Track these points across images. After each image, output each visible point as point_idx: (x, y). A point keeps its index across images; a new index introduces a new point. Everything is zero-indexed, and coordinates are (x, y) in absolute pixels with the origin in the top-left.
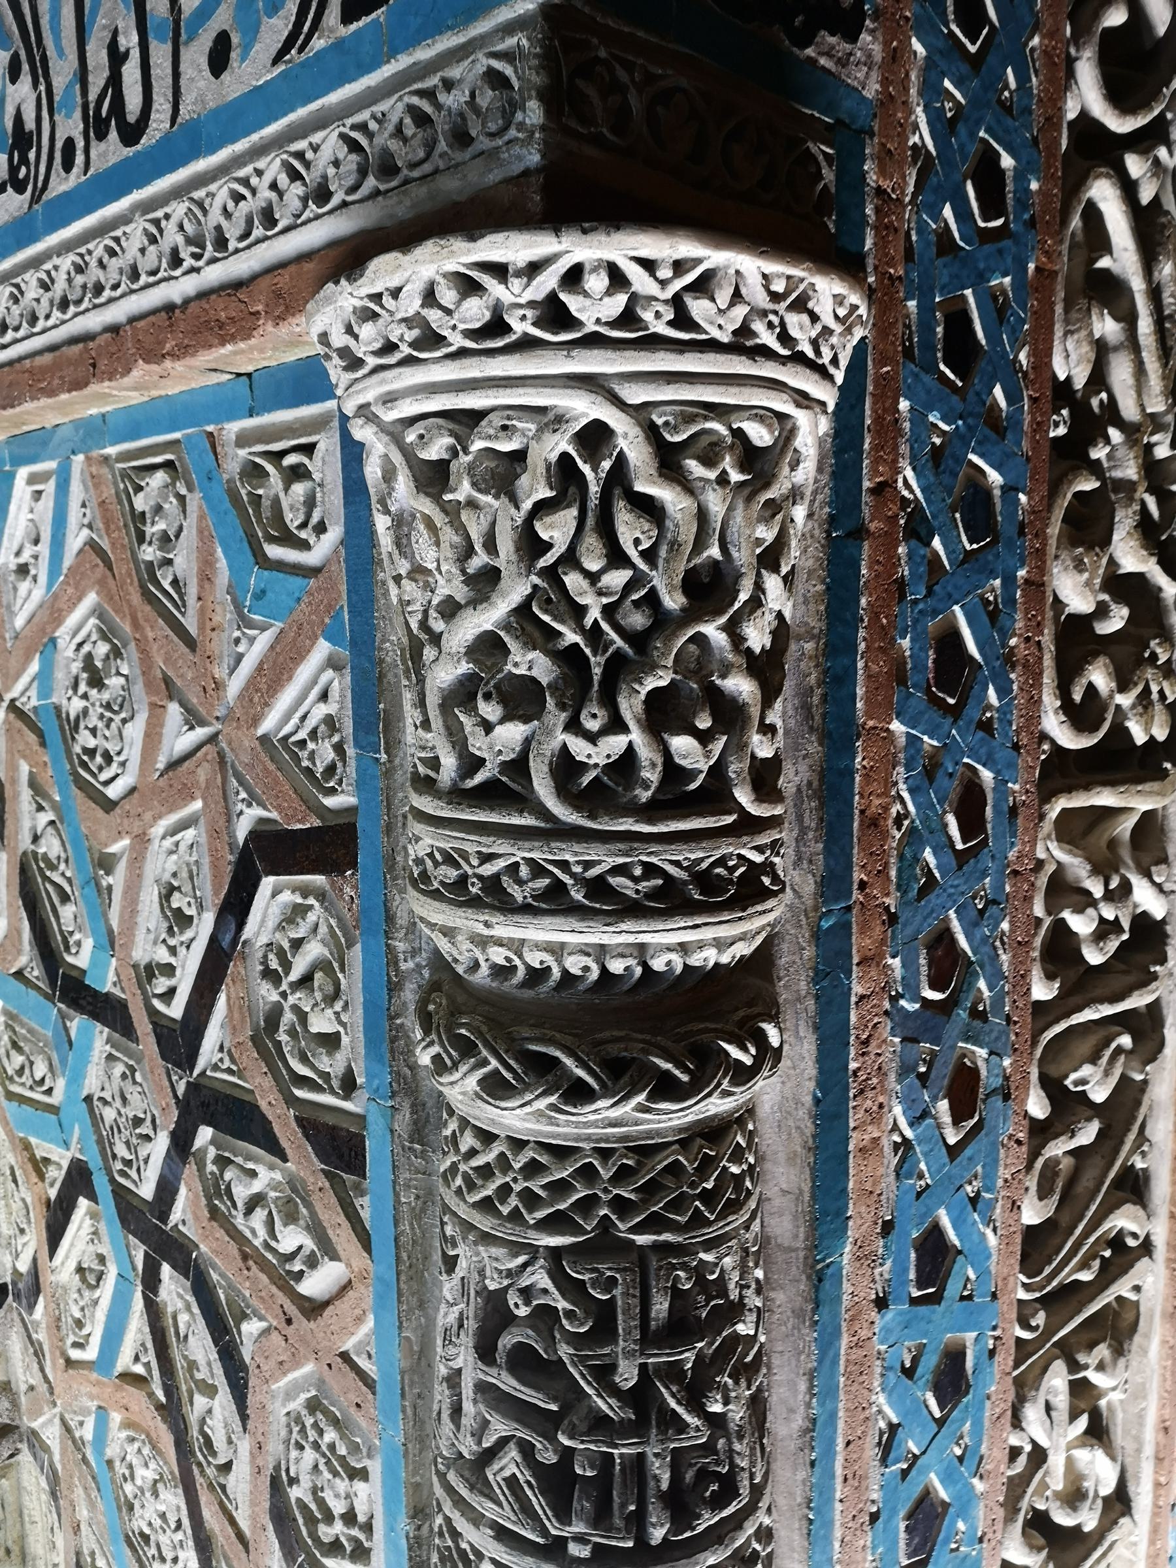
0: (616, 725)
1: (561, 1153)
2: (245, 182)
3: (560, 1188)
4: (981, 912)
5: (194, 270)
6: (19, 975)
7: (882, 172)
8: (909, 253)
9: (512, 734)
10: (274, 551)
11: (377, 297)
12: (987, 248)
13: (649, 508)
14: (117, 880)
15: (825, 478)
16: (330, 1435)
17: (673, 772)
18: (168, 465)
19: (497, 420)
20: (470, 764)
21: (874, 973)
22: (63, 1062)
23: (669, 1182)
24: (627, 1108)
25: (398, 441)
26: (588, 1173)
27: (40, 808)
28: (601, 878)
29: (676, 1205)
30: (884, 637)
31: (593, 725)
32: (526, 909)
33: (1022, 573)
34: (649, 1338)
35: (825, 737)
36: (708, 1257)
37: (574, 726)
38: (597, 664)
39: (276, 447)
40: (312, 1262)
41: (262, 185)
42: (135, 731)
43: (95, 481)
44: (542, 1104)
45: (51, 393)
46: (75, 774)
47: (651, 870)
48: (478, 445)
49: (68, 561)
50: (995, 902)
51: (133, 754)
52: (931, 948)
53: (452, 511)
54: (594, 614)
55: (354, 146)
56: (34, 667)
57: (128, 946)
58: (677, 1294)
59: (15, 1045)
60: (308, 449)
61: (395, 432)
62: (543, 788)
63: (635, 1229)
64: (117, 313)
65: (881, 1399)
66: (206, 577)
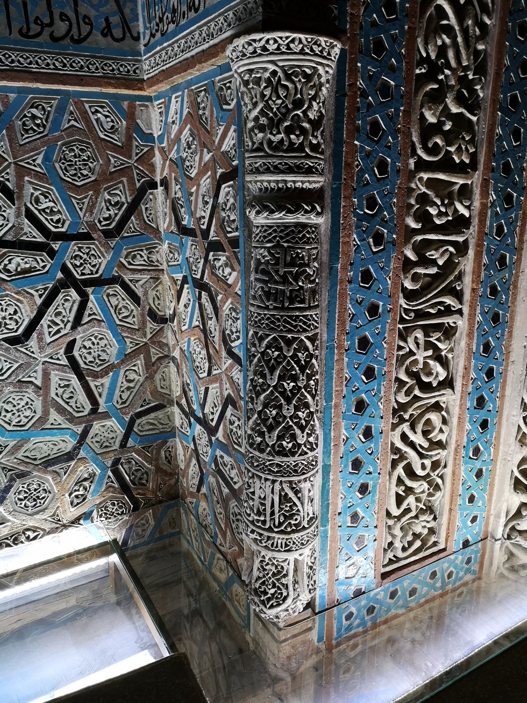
0: (279, 133)
1: (270, 227)
2: (217, 22)
3: (270, 234)
4: (386, 195)
5: (208, 42)
6: (172, 232)
7: (352, 9)
8: (361, 28)
9: (260, 135)
10: (225, 107)
11: (235, 47)
12: (389, 24)
13: (286, 87)
14: (193, 198)
15: (335, 82)
16: (234, 314)
17: (291, 143)
18: (205, 90)
19: (256, 70)
20: (254, 143)
21: (348, 201)
22: (181, 250)
23: (291, 233)
24: (281, 215)
25: (240, 76)
26: (275, 231)
27: (177, 185)
28: (276, 165)
29: (293, 238)
30: (352, 121)
31: (274, 132)
32: (263, 173)
33: (402, 108)
34: (286, 265)
35: (335, 142)
36: (299, 251)
37: (271, 133)
38: (276, 119)
39: (225, 82)
40: (230, 274)
41: (220, 22)
42: (197, 158)
43: (189, 96)
44: (265, 215)
45: (180, 73)
46: (185, 173)
47: (286, 164)
48: (253, 76)
49: (183, 118)
50: (391, 193)
51: (197, 164)
52: (367, 200)
53: (249, 89)
54: (275, 109)
55: (235, 15)
56: (176, 147)
57: (195, 214)
58: (292, 257)
59: (171, 252)
60: (230, 82)
61: (240, 74)
62: (266, 147)
63: (284, 242)
64: (193, 53)
65: (350, 306)
66: (212, 116)
